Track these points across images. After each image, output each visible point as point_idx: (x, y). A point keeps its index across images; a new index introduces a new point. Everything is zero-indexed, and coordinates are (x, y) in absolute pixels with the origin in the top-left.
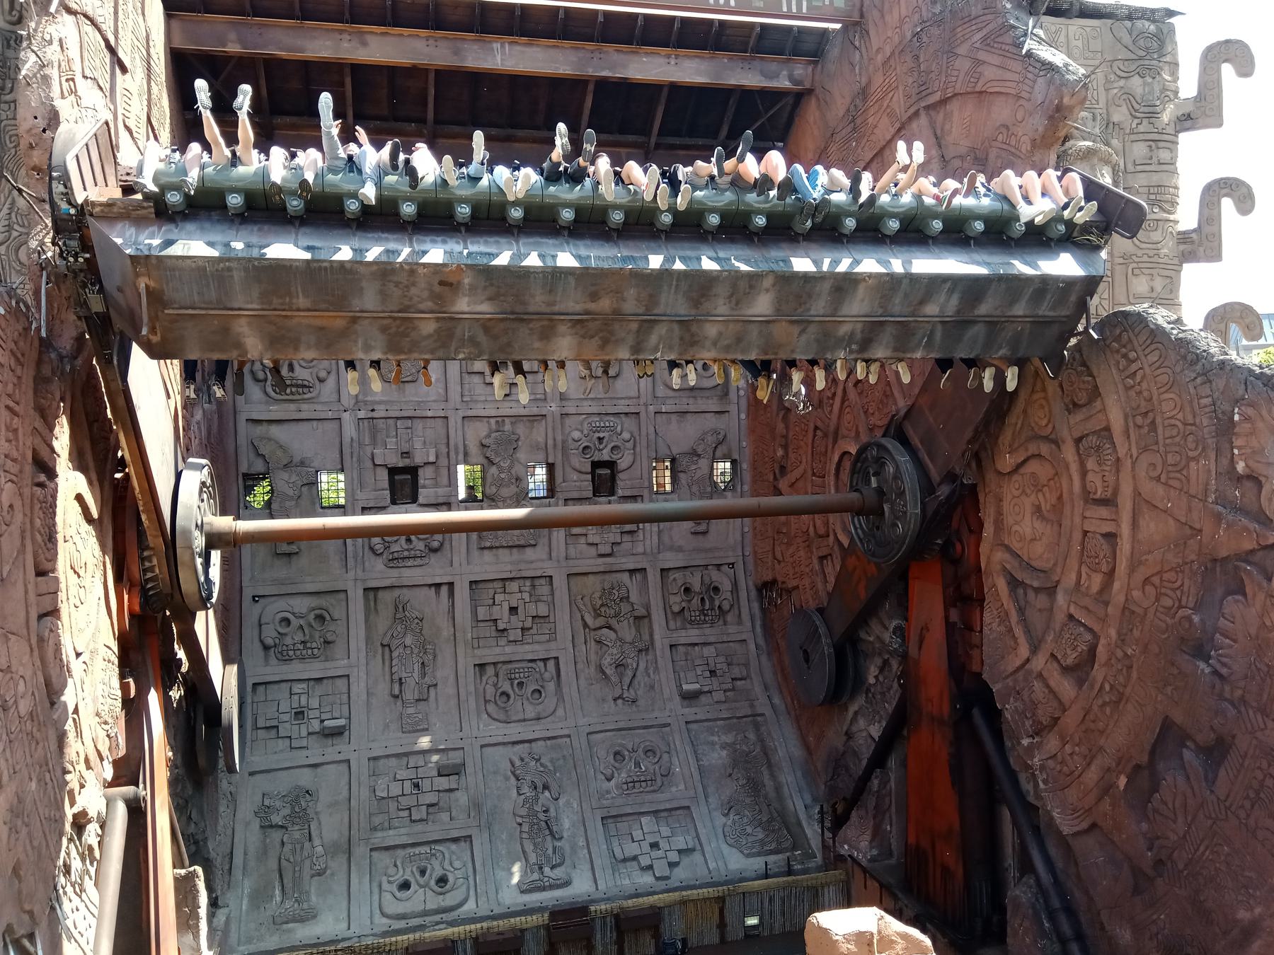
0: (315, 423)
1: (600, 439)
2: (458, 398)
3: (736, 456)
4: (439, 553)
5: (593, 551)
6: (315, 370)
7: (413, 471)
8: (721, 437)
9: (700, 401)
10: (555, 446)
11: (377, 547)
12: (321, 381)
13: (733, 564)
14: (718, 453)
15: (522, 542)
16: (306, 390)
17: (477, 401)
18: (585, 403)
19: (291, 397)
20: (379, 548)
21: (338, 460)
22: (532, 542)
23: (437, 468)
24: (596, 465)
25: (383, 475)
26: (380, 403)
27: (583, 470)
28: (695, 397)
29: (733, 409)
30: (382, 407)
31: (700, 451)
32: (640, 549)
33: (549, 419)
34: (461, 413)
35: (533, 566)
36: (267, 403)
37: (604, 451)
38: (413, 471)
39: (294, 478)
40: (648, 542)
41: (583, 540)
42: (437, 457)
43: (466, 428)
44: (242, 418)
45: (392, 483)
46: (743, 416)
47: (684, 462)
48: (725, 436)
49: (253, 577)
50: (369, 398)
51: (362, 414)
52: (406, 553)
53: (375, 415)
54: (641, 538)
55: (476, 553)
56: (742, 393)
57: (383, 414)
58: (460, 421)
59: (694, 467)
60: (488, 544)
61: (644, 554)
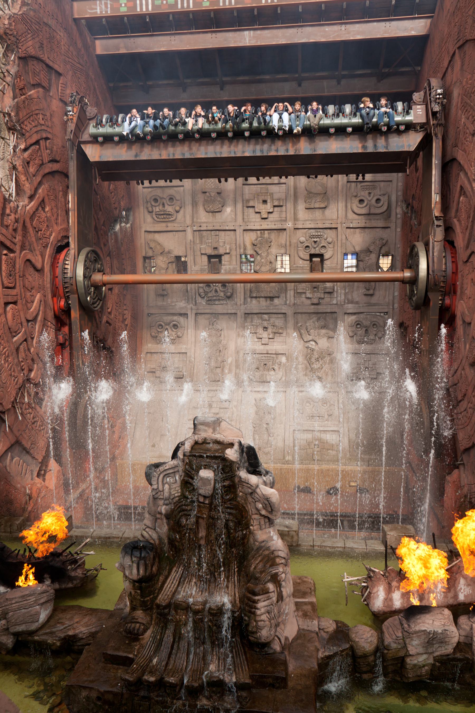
0: (174, 233)
1: (315, 242)
2: (241, 221)
3: (393, 253)
4: (231, 299)
5: (309, 302)
6: (174, 206)
7: (219, 257)
8: (384, 242)
9: (373, 221)
10: (290, 245)
11: (202, 294)
12: (177, 212)
13: (387, 313)
14: (383, 251)
15: (271, 295)
16: (170, 216)
17: (250, 222)
18: (308, 222)
19: (164, 220)
20: (203, 294)
21: (185, 251)
22: (277, 295)
23: (231, 256)
24: (312, 256)
25: (205, 259)
26: (204, 223)
27: (305, 258)
28: (370, 220)
29: (393, 225)
30: (205, 225)
31: (371, 249)
32: (335, 302)
33: (288, 231)
34: (243, 228)
35: (277, 307)
36: (154, 223)
37: (317, 249)
38: (219, 257)
39: (165, 259)
40: (339, 299)
41: (303, 296)
42: (231, 250)
43: (245, 235)
44: (143, 230)
45: (209, 261)
46: (399, 230)
47: (362, 256)
48: (387, 241)
49: (147, 305)
50: (199, 221)
51: (195, 228)
52: (215, 298)
53: (202, 229)
54: (336, 296)
55: (249, 300)
56: (399, 216)
57: (205, 228)
58: (242, 231)
59: (367, 258)
60: (255, 295)
61: (337, 304)
